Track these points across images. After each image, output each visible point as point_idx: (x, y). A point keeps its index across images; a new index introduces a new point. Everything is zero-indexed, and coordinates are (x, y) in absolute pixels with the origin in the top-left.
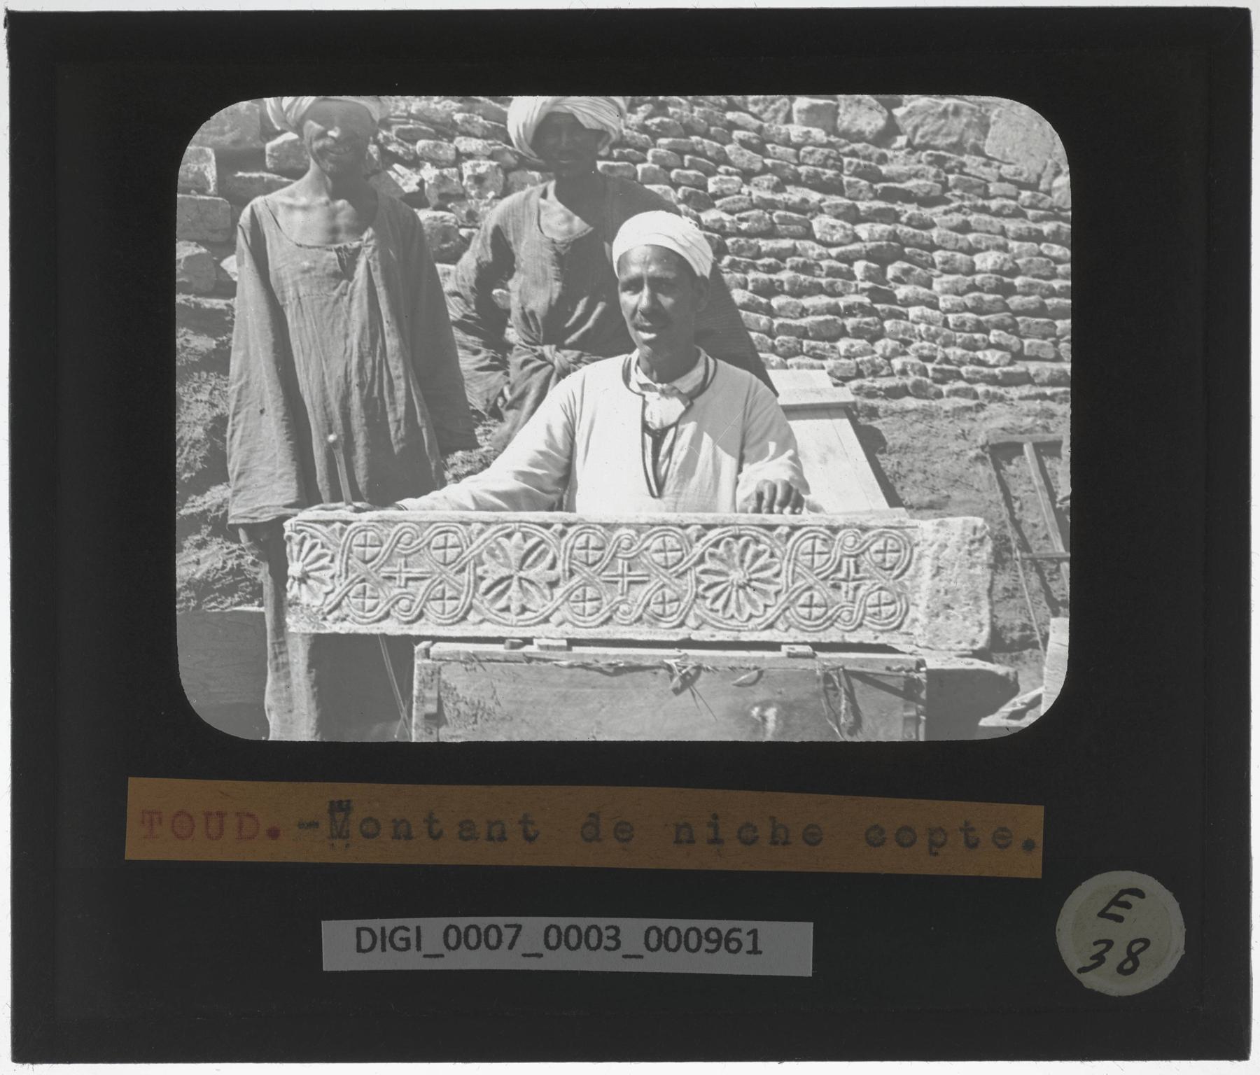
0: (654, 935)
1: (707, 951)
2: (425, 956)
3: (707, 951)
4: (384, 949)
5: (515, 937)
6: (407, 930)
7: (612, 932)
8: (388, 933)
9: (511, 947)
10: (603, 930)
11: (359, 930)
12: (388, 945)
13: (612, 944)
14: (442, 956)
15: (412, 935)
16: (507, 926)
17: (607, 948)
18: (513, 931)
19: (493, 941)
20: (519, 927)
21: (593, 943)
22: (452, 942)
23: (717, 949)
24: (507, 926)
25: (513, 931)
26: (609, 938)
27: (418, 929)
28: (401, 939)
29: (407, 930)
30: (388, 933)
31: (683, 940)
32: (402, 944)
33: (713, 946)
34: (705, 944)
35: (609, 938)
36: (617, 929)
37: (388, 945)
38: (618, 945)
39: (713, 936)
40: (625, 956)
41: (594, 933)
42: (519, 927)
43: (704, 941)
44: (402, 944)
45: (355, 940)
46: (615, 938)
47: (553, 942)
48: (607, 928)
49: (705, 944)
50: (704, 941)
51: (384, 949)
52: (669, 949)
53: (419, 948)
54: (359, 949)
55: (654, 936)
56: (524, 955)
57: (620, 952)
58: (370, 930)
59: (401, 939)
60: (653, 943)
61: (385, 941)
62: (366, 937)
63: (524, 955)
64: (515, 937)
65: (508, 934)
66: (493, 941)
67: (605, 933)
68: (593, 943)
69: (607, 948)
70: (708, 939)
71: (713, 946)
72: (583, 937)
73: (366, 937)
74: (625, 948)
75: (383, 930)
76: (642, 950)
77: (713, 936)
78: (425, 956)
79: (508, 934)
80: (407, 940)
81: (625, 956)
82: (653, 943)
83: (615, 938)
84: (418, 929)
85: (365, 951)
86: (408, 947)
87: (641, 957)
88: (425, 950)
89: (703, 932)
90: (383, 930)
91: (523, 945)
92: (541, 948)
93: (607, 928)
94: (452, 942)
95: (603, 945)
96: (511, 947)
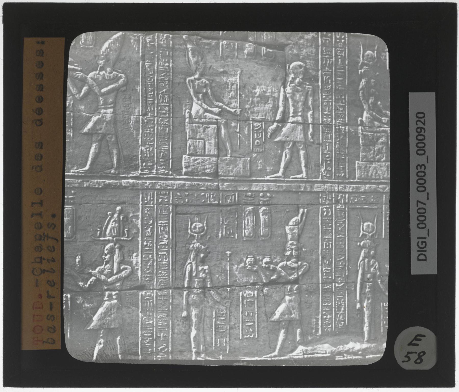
0: (419, 152)
1: (424, 132)
2: (428, 236)
3: (424, 132)
4: (426, 251)
5: (421, 203)
6: (418, 242)
7: (419, 167)
8: (421, 250)
9: (425, 204)
10: (417, 171)
11: (419, 260)
12: (423, 250)
13: (423, 167)
14: (428, 230)
15: (421, 240)
16: (417, 206)
17: (425, 169)
18: (419, 203)
19: (422, 211)
20: (418, 201)
21: (423, 174)
22: (423, 226)
23: (424, 129)
24: (417, 206)
25: (419, 203)
26: (421, 168)
27: (418, 238)
28: (422, 244)
29: (418, 242)
30: (421, 250)
31: (421, 141)
32: (424, 244)
33: (423, 130)
34: (422, 133)
35: (421, 168)
36: (418, 165)
37: (423, 250)
38: (423, 165)
39: (419, 130)
40: (428, 163)
42: (418, 201)
43: (421, 133)
44: (424, 244)
45: (421, 262)
46: (421, 166)
47: (423, 189)
48: (417, 169)
49: (422, 133)
50: (421, 133)
51: (426, 251)
52: (424, 147)
53: (425, 238)
54: (425, 260)
55: (420, 152)
56: (428, 199)
58: (419, 256)
59: (422, 244)
60: (422, 152)
61: (422, 250)
62: (421, 257)
63: (428, 199)
64: (421, 203)
65: (420, 205)
66: (422, 211)
67: (419, 170)
68: (423, 174)
69: (425, 169)
70: (421, 132)
71: (423, 130)
72: (421, 178)
73: (421, 257)
75: (418, 251)
76: (424, 157)
77: (419, 130)
78: (428, 236)
79: (420, 205)
80: (422, 242)
81: (428, 163)
82: (422, 152)
84: (418, 238)
85: (426, 258)
86: (425, 242)
87: (428, 156)
88: (426, 236)
89: (417, 134)
90: (418, 251)
91: (424, 200)
92: (425, 194)
93: (417, 169)
94: (423, 226)
96: (425, 204)
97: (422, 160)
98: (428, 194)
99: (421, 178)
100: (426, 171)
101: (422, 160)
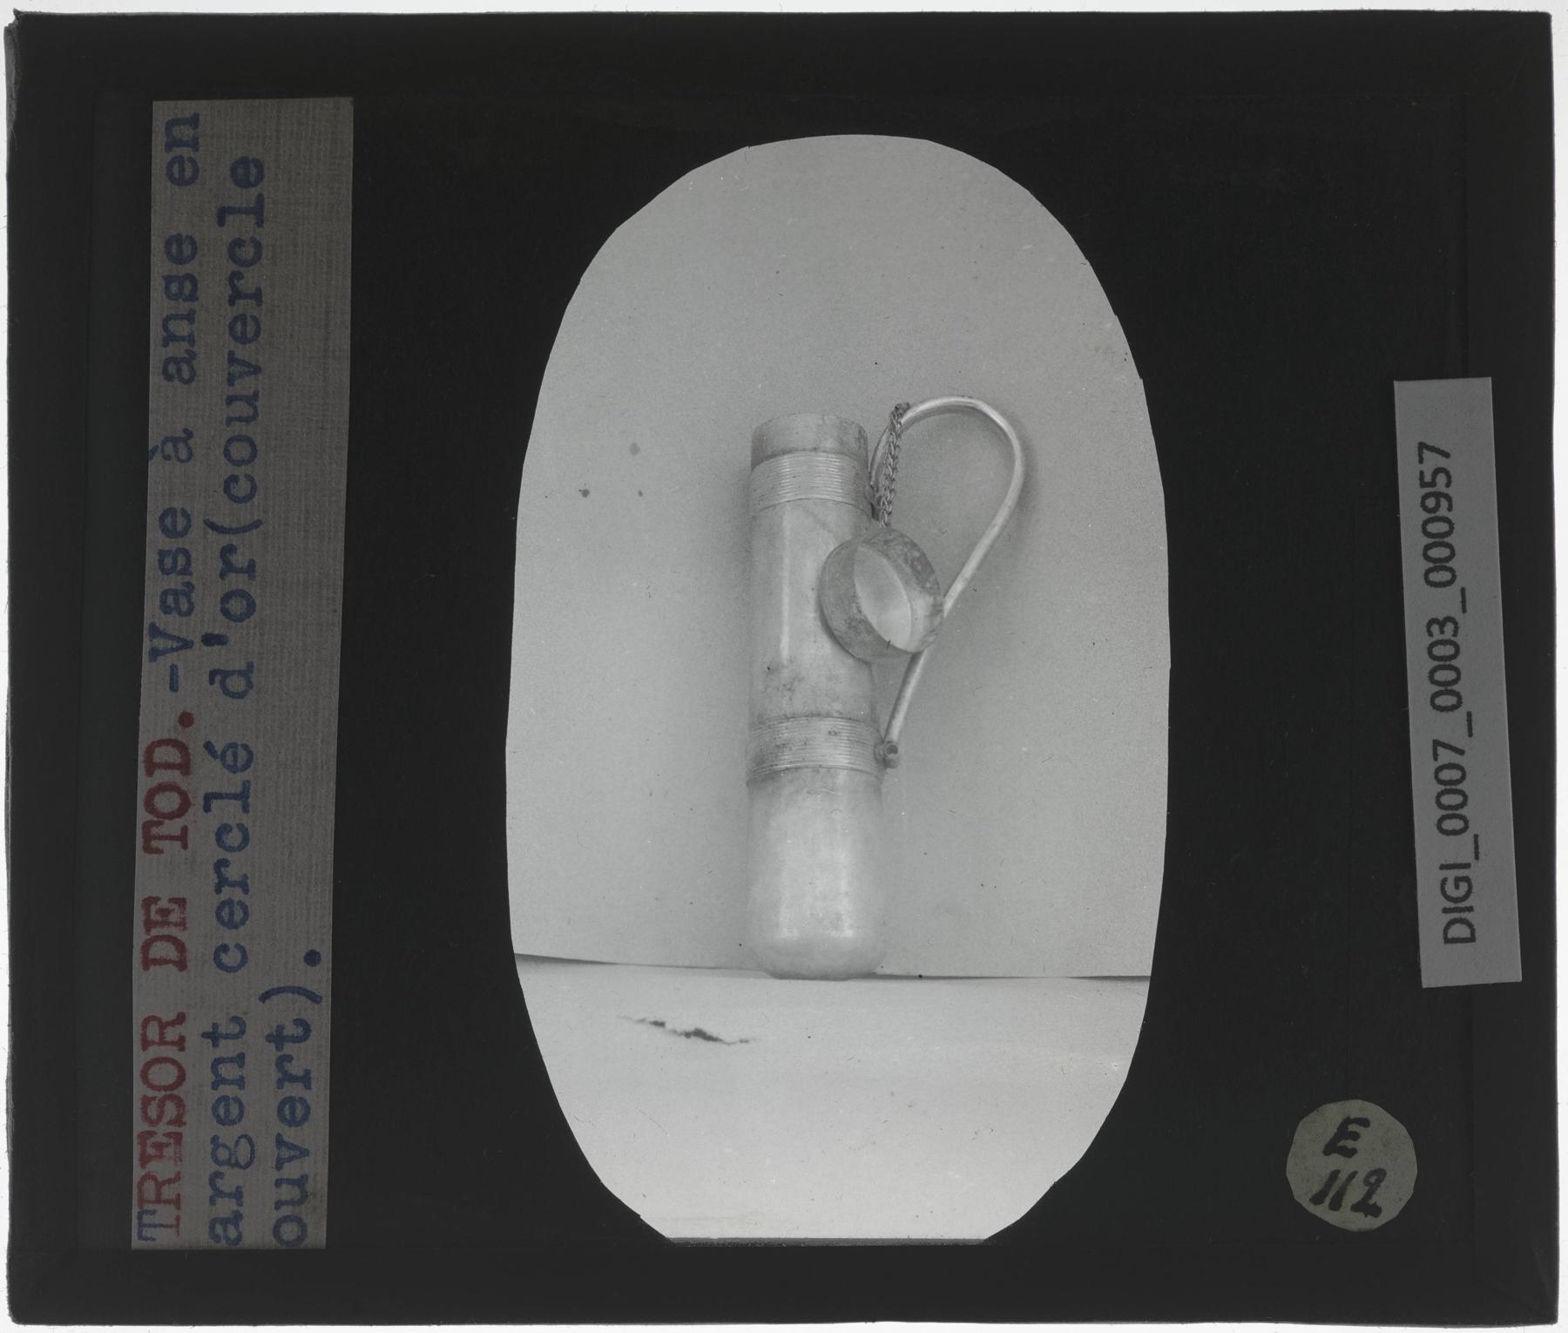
7: (1435, 629)
10: (1434, 639)
13: (1449, 627)
17: (1455, 633)
21: (1449, 650)
26: (1442, 632)
35: (1442, 632)
38: (1449, 619)
41: (1440, 651)
48: (1431, 634)
57: (1458, 616)
67: (1437, 636)
68: (1449, 650)
69: (1455, 633)
72: (1445, 663)
74: (1455, 612)
76: (1454, 590)
83: (1442, 624)
93: (1431, 634)
95: (1452, 638)
97: (1443, 602)
98: (1469, 715)
99: (1445, 663)
100: (1458, 640)
101: (1443, 602)
